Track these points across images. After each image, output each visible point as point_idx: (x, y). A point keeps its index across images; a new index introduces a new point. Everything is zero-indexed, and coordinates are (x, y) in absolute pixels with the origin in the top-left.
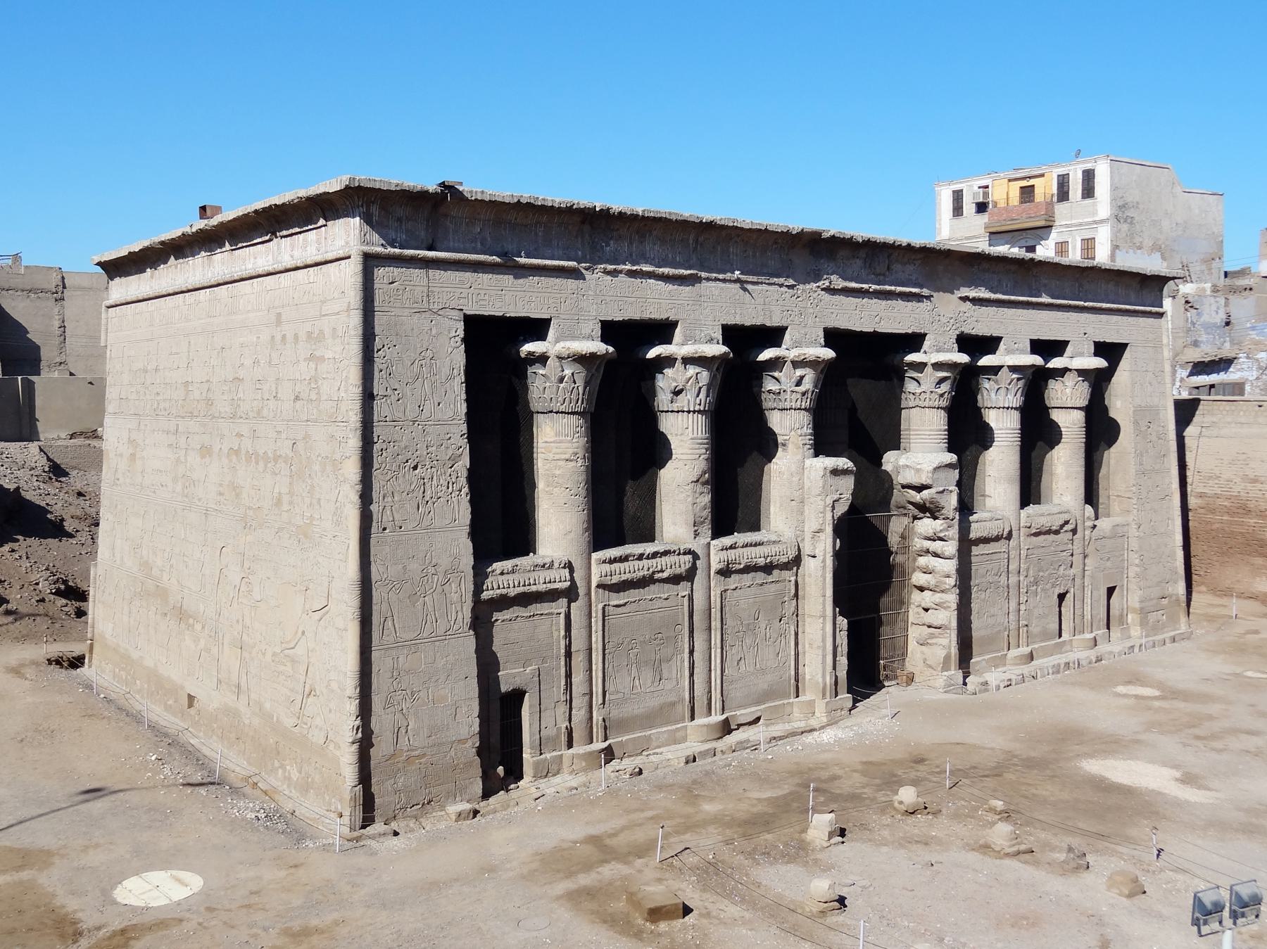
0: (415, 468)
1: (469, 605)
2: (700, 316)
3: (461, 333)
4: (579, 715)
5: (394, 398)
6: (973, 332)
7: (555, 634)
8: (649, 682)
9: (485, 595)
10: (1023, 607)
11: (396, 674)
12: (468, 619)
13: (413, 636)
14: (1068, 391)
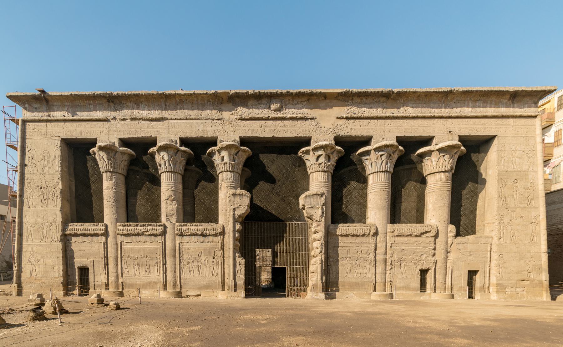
0: (41, 188)
1: (60, 234)
2: (384, 130)
3: (59, 144)
4: (112, 278)
5: (34, 166)
6: (348, 135)
7: (100, 250)
8: (144, 273)
9: (67, 232)
10: (388, 272)
11: (32, 253)
12: (59, 239)
13: (37, 241)
14: (434, 163)
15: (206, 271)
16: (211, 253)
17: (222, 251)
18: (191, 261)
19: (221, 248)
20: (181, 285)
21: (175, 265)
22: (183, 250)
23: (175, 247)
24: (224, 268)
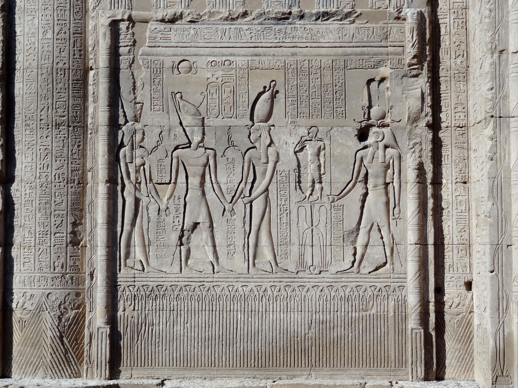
15: (306, 228)
16: (341, 93)
17: (422, 83)
18: (195, 158)
19: (420, 57)
20: (115, 338)
21: (80, 183)
22: (142, 75)
23: (82, 52)
24: (438, 210)
